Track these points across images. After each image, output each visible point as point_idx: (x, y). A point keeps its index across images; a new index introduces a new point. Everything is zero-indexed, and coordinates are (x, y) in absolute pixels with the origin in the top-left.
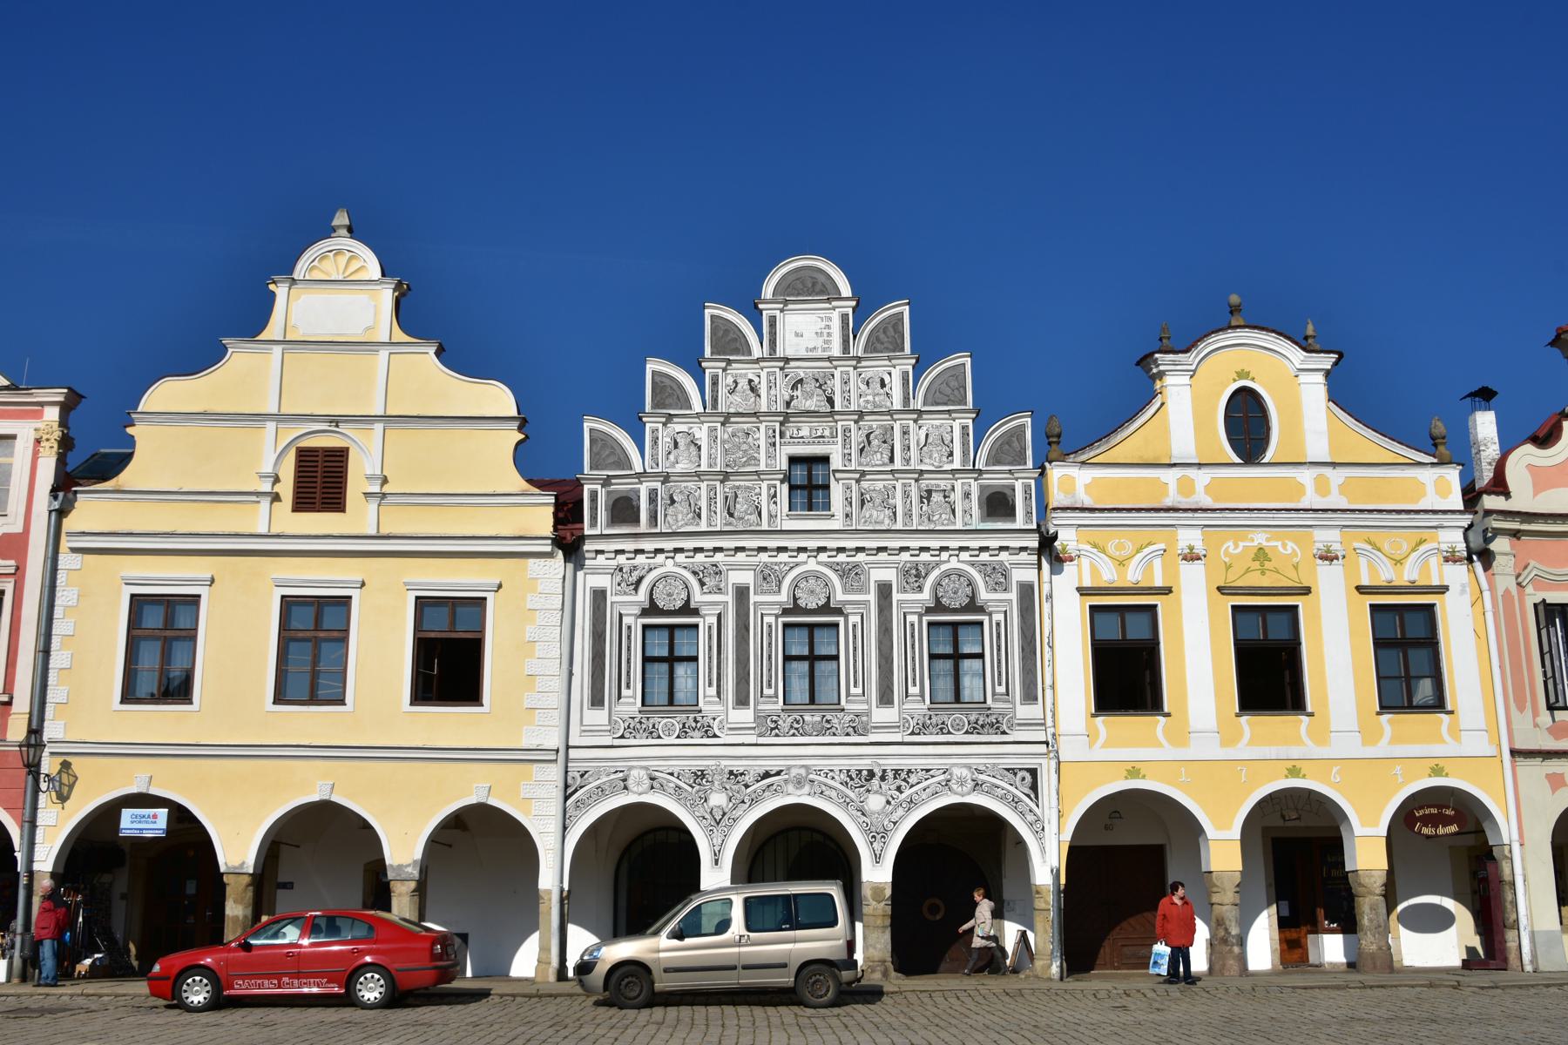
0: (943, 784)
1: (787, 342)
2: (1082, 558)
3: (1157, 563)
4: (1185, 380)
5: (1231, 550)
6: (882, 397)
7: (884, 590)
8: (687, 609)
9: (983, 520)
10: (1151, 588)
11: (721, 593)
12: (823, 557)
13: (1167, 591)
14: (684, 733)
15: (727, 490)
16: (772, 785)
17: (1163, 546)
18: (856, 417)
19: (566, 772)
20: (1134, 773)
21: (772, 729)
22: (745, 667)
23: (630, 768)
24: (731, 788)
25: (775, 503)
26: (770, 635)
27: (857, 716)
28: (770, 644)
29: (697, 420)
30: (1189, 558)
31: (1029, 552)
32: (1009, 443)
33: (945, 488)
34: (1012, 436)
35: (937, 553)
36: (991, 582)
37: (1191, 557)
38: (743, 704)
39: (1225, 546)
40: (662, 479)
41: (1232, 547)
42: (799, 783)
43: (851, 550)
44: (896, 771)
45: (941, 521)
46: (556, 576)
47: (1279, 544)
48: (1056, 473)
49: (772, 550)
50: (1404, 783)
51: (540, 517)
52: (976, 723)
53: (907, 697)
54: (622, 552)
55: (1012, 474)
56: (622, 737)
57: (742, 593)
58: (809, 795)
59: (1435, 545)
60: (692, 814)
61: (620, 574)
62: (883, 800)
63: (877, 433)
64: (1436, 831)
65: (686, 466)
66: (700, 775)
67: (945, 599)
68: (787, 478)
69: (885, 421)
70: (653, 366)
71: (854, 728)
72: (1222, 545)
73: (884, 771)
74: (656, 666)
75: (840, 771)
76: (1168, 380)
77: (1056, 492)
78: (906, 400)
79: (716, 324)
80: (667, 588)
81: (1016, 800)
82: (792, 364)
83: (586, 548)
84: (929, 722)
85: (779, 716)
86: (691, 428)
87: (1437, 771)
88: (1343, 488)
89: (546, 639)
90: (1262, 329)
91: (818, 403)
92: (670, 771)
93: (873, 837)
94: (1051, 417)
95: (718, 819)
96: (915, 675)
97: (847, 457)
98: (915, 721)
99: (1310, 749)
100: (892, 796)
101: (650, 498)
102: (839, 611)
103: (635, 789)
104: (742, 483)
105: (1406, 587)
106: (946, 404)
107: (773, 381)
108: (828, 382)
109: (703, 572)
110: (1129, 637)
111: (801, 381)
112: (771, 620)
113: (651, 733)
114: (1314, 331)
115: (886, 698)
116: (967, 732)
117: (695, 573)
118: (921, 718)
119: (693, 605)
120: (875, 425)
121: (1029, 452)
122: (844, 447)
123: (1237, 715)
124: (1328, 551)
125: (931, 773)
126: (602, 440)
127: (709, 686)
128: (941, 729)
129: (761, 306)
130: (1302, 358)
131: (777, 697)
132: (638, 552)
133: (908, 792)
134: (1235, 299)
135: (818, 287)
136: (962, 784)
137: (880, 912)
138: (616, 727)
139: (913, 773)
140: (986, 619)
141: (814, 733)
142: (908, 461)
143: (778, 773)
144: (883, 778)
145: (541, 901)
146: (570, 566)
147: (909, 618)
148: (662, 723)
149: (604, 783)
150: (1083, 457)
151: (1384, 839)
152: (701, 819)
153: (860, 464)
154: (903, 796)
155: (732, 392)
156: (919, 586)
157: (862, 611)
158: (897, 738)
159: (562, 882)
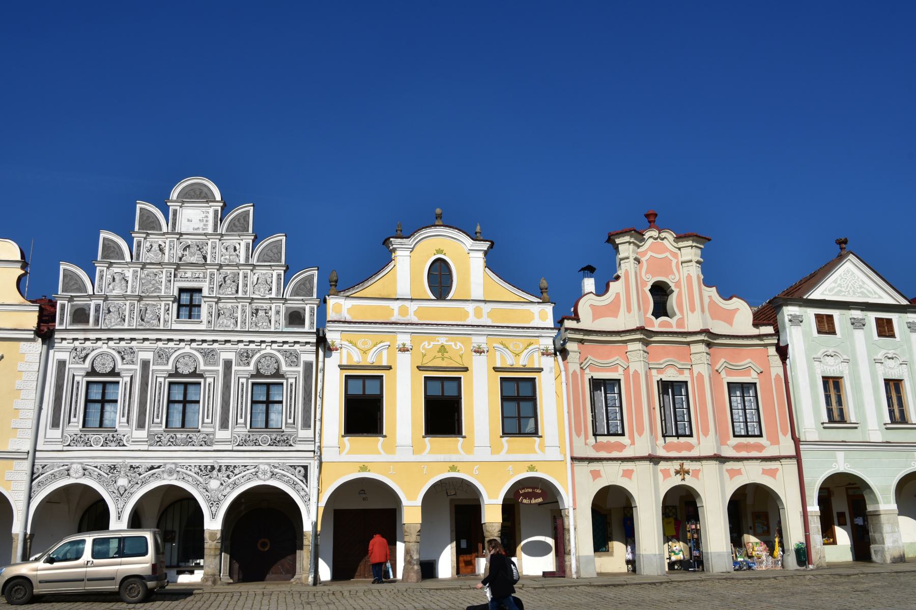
0: (254, 474)
1: (182, 225)
2: (343, 349)
3: (385, 353)
4: (408, 253)
5: (426, 346)
6: (234, 257)
7: (228, 364)
8: (113, 373)
9: (286, 327)
10: (379, 366)
12: (194, 345)
13: (389, 368)
14: (106, 443)
15: (141, 306)
16: (155, 474)
17: (388, 343)
18: (218, 267)
19: (33, 465)
20: (364, 468)
21: (158, 442)
22: (144, 406)
23: (72, 463)
24: (130, 475)
25: (168, 314)
26: (160, 388)
27: (207, 435)
28: (160, 393)
29: (127, 266)
30: (402, 350)
31: (311, 345)
33: (266, 308)
34: (306, 280)
35: (259, 344)
36: (289, 361)
37: (404, 350)
38: (141, 427)
39: (423, 344)
40: (103, 298)
41: (427, 345)
42: (171, 473)
43: (210, 341)
44: (227, 466)
45: (263, 326)
46: (36, 352)
47: (453, 343)
48: (332, 301)
49: (164, 340)
50: (513, 475)
51: (30, 318)
52: (275, 440)
53: (237, 424)
54: (77, 339)
55: (304, 301)
56: (69, 445)
57: (145, 364)
59: (538, 346)
60: (107, 490)
61: (75, 352)
62: (218, 483)
63: (230, 276)
64: (530, 501)
65: (119, 292)
66: (113, 468)
68: (177, 300)
69: (235, 270)
70: (104, 235)
72: (421, 344)
73: (220, 466)
74: (176, 405)
75: (195, 466)
76: (398, 253)
77: (331, 311)
78: (247, 259)
80: (102, 361)
81: (295, 483)
82: (184, 236)
83: (56, 336)
84: (248, 439)
85: (162, 434)
86: (123, 270)
87: (532, 469)
88: (490, 315)
89: (28, 388)
90: (450, 227)
91: (198, 259)
92: (95, 465)
93: (212, 504)
94: (333, 271)
95: (122, 493)
97: (211, 289)
98: (241, 438)
99: (463, 456)
100: (224, 481)
101: (96, 309)
103: (74, 476)
104: (150, 302)
105: (520, 368)
106: (270, 262)
107: (172, 246)
108: (204, 247)
109: (124, 352)
110: (366, 393)
111: (189, 246)
112: (162, 380)
113: (86, 443)
114: (480, 229)
115: (224, 425)
116: (270, 445)
117: (119, 352)
118: (244, 436)
119: (117, 371)
120: (229, 272)
121: (315, 290)
122: (210, 283)
123: (424, 437)
124: (479, 348)
125: (247, 467)
126: (70, 275)
127: (123, 417)
129: (168, 204)
130: (471, 244)
131: (161, 423)
132: (86, 339)
133: (233, 478)
134: (438, 211)
135: (203, 195)
136: (264, 474)
137: (213, 547)
138: (66, 439)
139: (237, 467)
140: (285, 381)
141: (182, 445)
142: (246, 292)
143: (159, 467)
144: (219, 470)
145: (14, 541)
146: (45, 347)
147: (241, 380)
148: (93, 437)
149: (56, 472)
150: (348, 294)
151: (501, 506)
152: (112, 493)
153: (219, 294)
155: (149, 251)
156: (248, 363)
158: (230, 448)
159: (26, 528)
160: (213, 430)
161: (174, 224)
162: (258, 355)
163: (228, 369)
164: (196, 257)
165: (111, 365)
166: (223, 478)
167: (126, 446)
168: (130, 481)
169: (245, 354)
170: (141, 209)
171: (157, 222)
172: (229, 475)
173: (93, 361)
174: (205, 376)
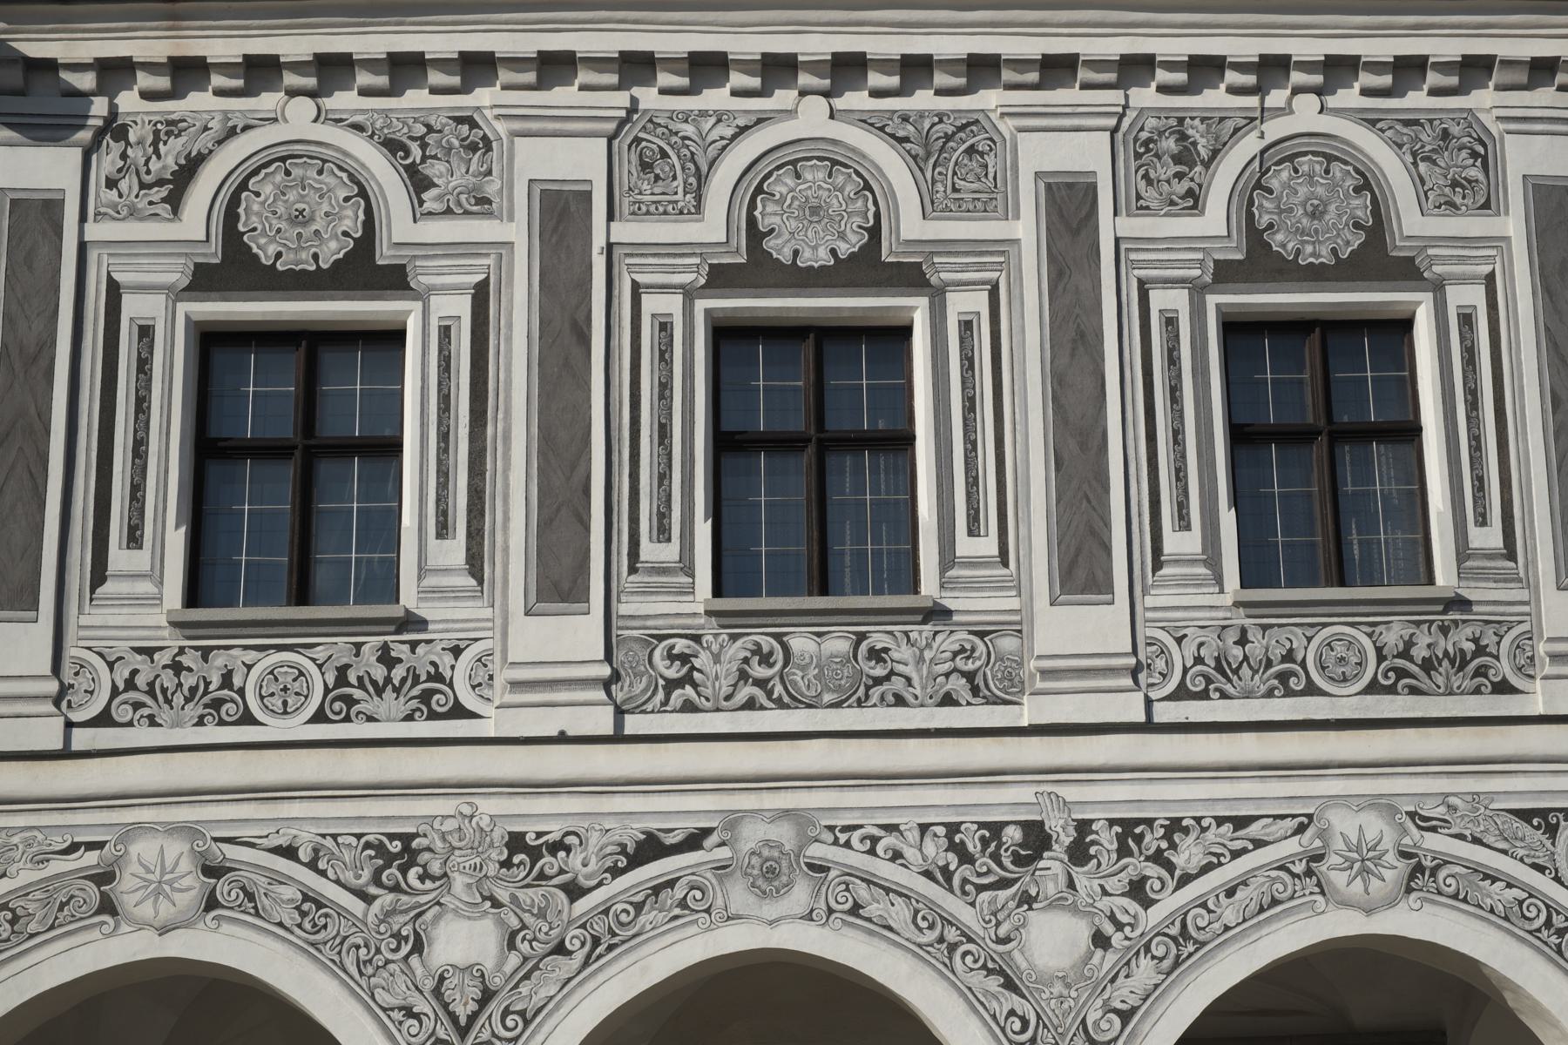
0: (1299, 868)
11: (489, 214)
21: (672, 685)
22: (573, 467)
26: (664, 356)
27: (982, 635)
28: (664, 388)
38: (565, 597)
44: (1128, 825)
53: (1157, 565)
58: (809, 917)
67: (1280, 237)
71: (970, 676)
73: (1084, 827)
75: (924, 828)
80: (292, 196)
84: (1237, 652)
85: (697, 639)
96: (1185, 492)
98: (1190, 649)
100: (1112, 918)
102: (911, 278)
116: (1373, 688)
117: (393, 146)
118: (1211, 637)
119: (385, 255)
125: (1254, 830)
128: (1283, 677)
131: (686, 566)
133: (1169, 903)
141: (828, 698)
143: (694, 841)
144: (1079, 853)
147: (1160, 300)
154: (1156, 915)
156: (1190, 193)
157: (995, 275)
160: (1014, 603)
162: (1249, 146)
163: (1075, 232)
165: (347, 224)
166: (1104, 903)
167: (473, 715)
168: (513, 935)
169: (1170, 144)
172: (1144, 879)
173: (234, 201)
174: (934, 280)
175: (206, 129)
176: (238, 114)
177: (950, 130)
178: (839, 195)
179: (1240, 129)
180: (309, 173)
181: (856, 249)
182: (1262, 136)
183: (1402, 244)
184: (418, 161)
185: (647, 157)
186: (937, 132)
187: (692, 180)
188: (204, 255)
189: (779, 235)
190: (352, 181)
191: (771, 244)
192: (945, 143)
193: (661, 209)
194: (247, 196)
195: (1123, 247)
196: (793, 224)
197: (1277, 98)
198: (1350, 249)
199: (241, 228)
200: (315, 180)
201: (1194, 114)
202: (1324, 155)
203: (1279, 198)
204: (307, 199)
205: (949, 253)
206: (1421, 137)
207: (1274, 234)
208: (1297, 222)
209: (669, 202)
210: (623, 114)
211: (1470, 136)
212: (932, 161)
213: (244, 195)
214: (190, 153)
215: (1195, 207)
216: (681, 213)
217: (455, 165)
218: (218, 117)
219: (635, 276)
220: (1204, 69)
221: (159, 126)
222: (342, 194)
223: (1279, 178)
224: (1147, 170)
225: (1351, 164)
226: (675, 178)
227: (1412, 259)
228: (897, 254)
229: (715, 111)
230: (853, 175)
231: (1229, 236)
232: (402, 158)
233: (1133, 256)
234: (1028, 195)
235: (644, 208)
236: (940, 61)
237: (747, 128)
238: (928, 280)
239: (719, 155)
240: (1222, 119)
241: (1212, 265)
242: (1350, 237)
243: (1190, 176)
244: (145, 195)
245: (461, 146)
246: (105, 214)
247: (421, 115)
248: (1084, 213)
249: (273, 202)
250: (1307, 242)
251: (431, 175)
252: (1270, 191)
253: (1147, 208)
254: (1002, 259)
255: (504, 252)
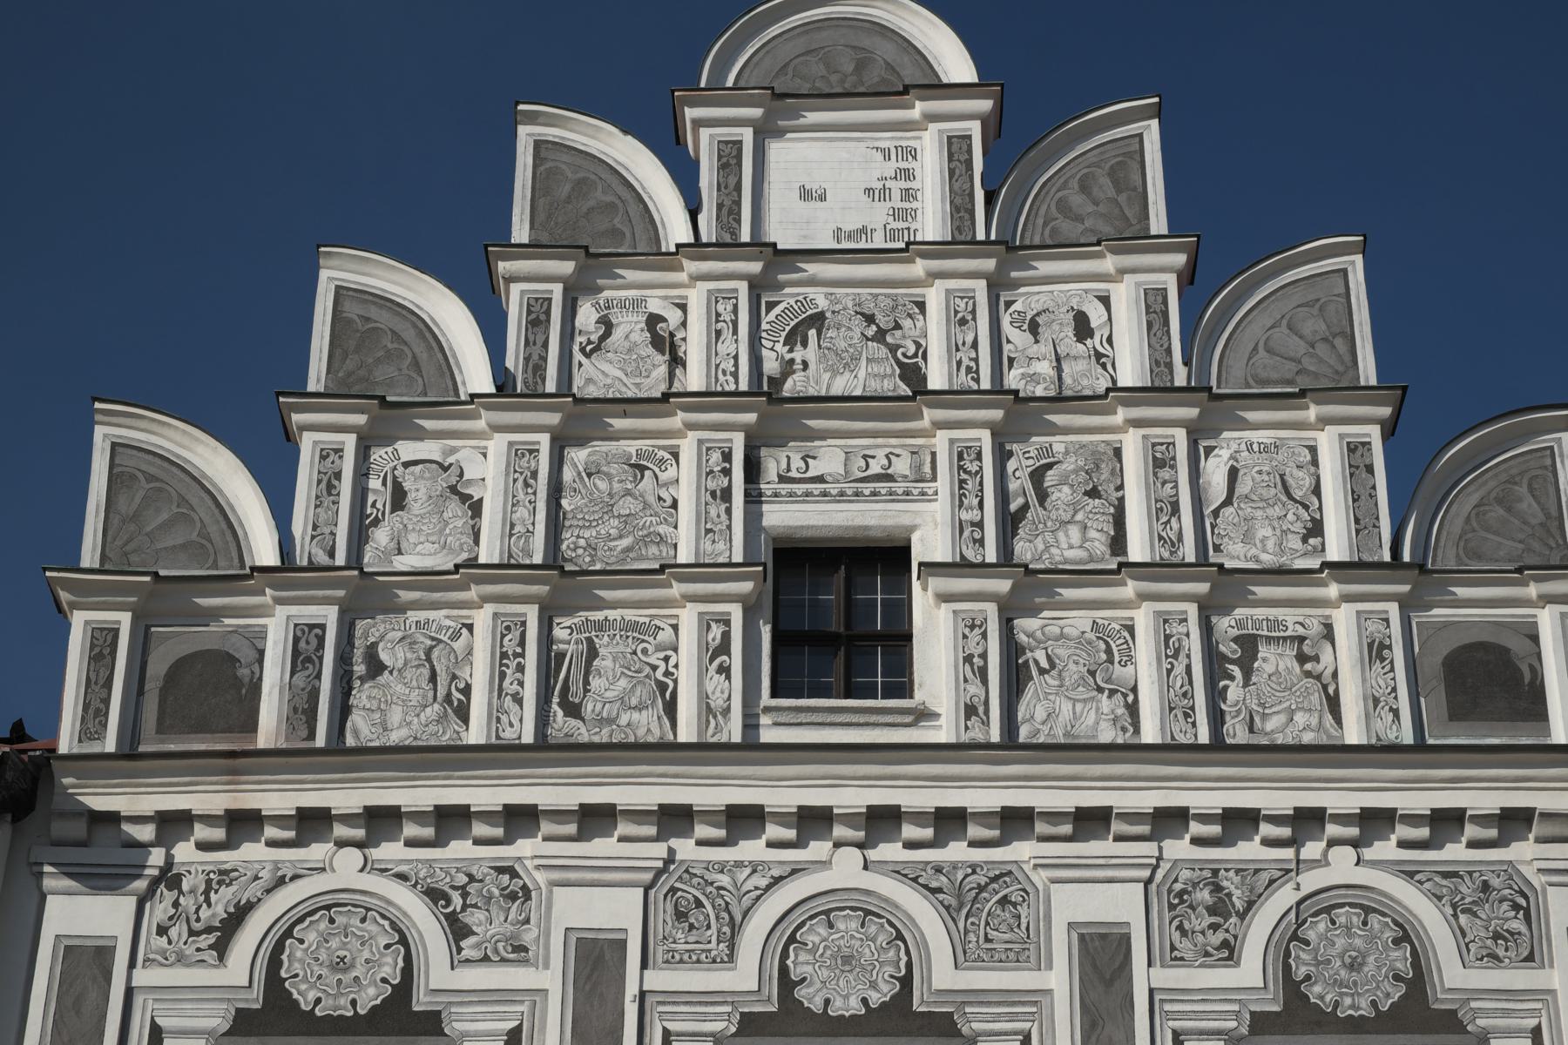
6: (1081, 366)
11: (525, 962)
25: (725, 670)
32: (1506, 501)
33: (1301, 631)
34: (1512, 481)
63: (1068, 465)
67: (1317, 989)
79: (548, 165)
80: (334, 943)
86: (454, 450)
101: (296, 652)
106: (1290, 382)
108: (907, 323)
111: (818, 320)
117: (435, 895)
119: (421, 1002)
156: (1225, 944)
161: (729, 212)
162: (1285, 897)
163: (1109, 983)
164: (862, 374)
165: (386, 971)
170: (539, 145)
171: (634, 210)
173: (279, 947)
174: (965, 1030)
175: (256, 878)
176: (288, 864)
177: (983, 880)
178: (871, 945)
179: (1275, 880)
180: (352, 922)
181: (888, 999)
182: (1298, 888)
183: (1444, 996)
184: (458, 910)
185: (682, 906)
186: (970, 883)
187: (726, 929)
188: (247, 1000)
189: (808, 986)
190: (393, 929)
191: (803, 992)
192: (978, 894)
193: (694, 958)
194: (292, 943)
195: (1157, 997)
196: (825, 973)
197: (1312, 850)
198: (1390, 1001)
199: (283, 974)
200: (357, 928)
201: (1229, 866)
202: (1361, 906)
203: (1316, 950)
204: (349, 946)
205: (981, 1003)
206: (1462, 890)
207: (1311, 985)
208: (1335, 974)
209: (703, 951)
210: (660, 864)
211: (1511, 888)
212: (965, 911)
213: (288, 942)
214: (239, 901)
215: (1230, 958)
216: (714, 961)
217: (494, 914)
218: (269, 867)
219: (666, 1024)
220: (1239, 822)
221: (212, 875)
222: (383, 941)
223: (1316, 930)
224: (1181, 921)
225: (1390, 916)
226: (709, 927)
227: (1454, 1012)
228: (928, 1006)
229: (750, 862)
230: (886, 925)
231: (1265, 987)
232: (443, 907)
233: (1167, 1007)
234: (1061, 946)
235: (677, 957)
236: (974, 814)
237: (781, 878)
238: (959, 1030)
239: (753, 905)
240: (1257, 871)
241: (1248, 1016)
242: (1390, 990)
243: (1225, 927)
244: (194, 941)
245: (501, 895)
246: (154, 960)
247: (464, 865)
248: (1117, 964)
249: (317, 948)
250: (1346, 994)
251: (470, 923)
252: (1307, 943)
253: (1182, 959)
254: (1034, 1010)
255: (537, 999)
